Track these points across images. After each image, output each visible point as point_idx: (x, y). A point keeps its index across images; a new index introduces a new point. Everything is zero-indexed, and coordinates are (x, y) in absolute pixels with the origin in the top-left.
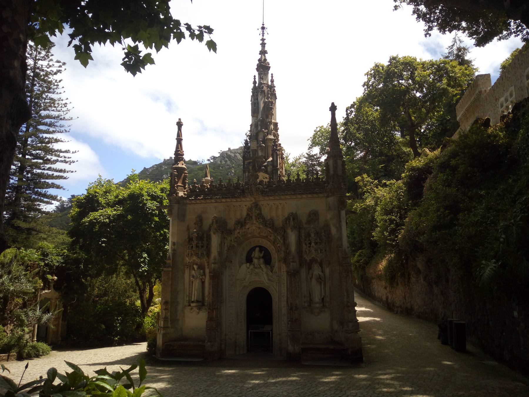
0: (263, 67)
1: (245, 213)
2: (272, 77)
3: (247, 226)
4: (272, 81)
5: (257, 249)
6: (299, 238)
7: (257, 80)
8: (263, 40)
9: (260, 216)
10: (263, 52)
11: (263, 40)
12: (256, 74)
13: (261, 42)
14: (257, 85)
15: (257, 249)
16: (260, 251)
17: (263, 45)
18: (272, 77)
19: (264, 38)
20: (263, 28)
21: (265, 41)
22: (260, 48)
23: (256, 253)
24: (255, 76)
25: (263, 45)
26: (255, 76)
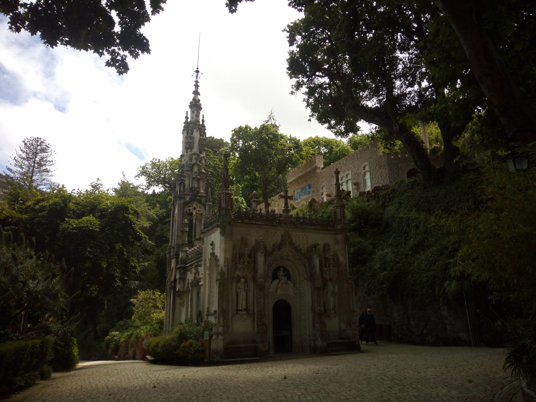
0: (196, 106)
1: (279, 240)
2: (203, 117)
3: (283, 250)
4: (203, 121)
5: (282, 269)
6: (320, 262)
7: (189, 116)
8: (197, 82)
9: (291, 243)
10: (196, 93)
11: (197, 82)
12: (189, 110)
13: (195, 83)
14: (189, 120)
15: (282, 269)
16: (284, 271)
17: (197, 86)
18: (203, 117)
19: (198, 80)
20: (197, 72)
21: (198, 84)
22: (194, 89)
23: (281, 273)
24: (187, 112)
25: (197, 86)
26: (187, 112)
